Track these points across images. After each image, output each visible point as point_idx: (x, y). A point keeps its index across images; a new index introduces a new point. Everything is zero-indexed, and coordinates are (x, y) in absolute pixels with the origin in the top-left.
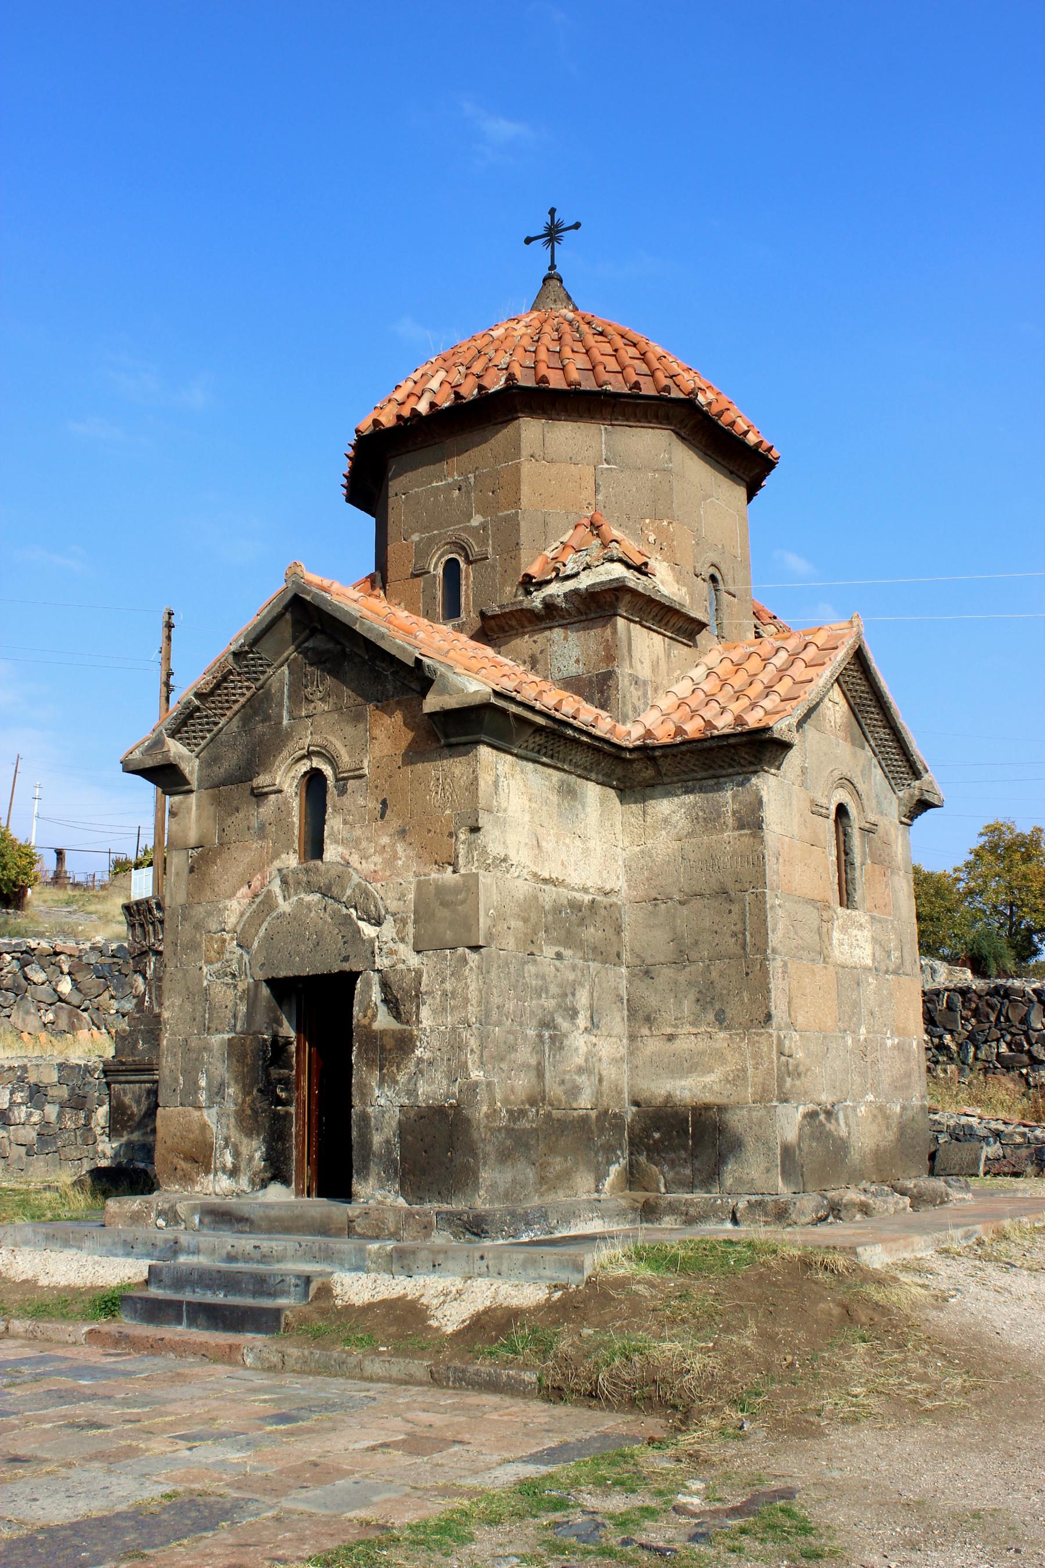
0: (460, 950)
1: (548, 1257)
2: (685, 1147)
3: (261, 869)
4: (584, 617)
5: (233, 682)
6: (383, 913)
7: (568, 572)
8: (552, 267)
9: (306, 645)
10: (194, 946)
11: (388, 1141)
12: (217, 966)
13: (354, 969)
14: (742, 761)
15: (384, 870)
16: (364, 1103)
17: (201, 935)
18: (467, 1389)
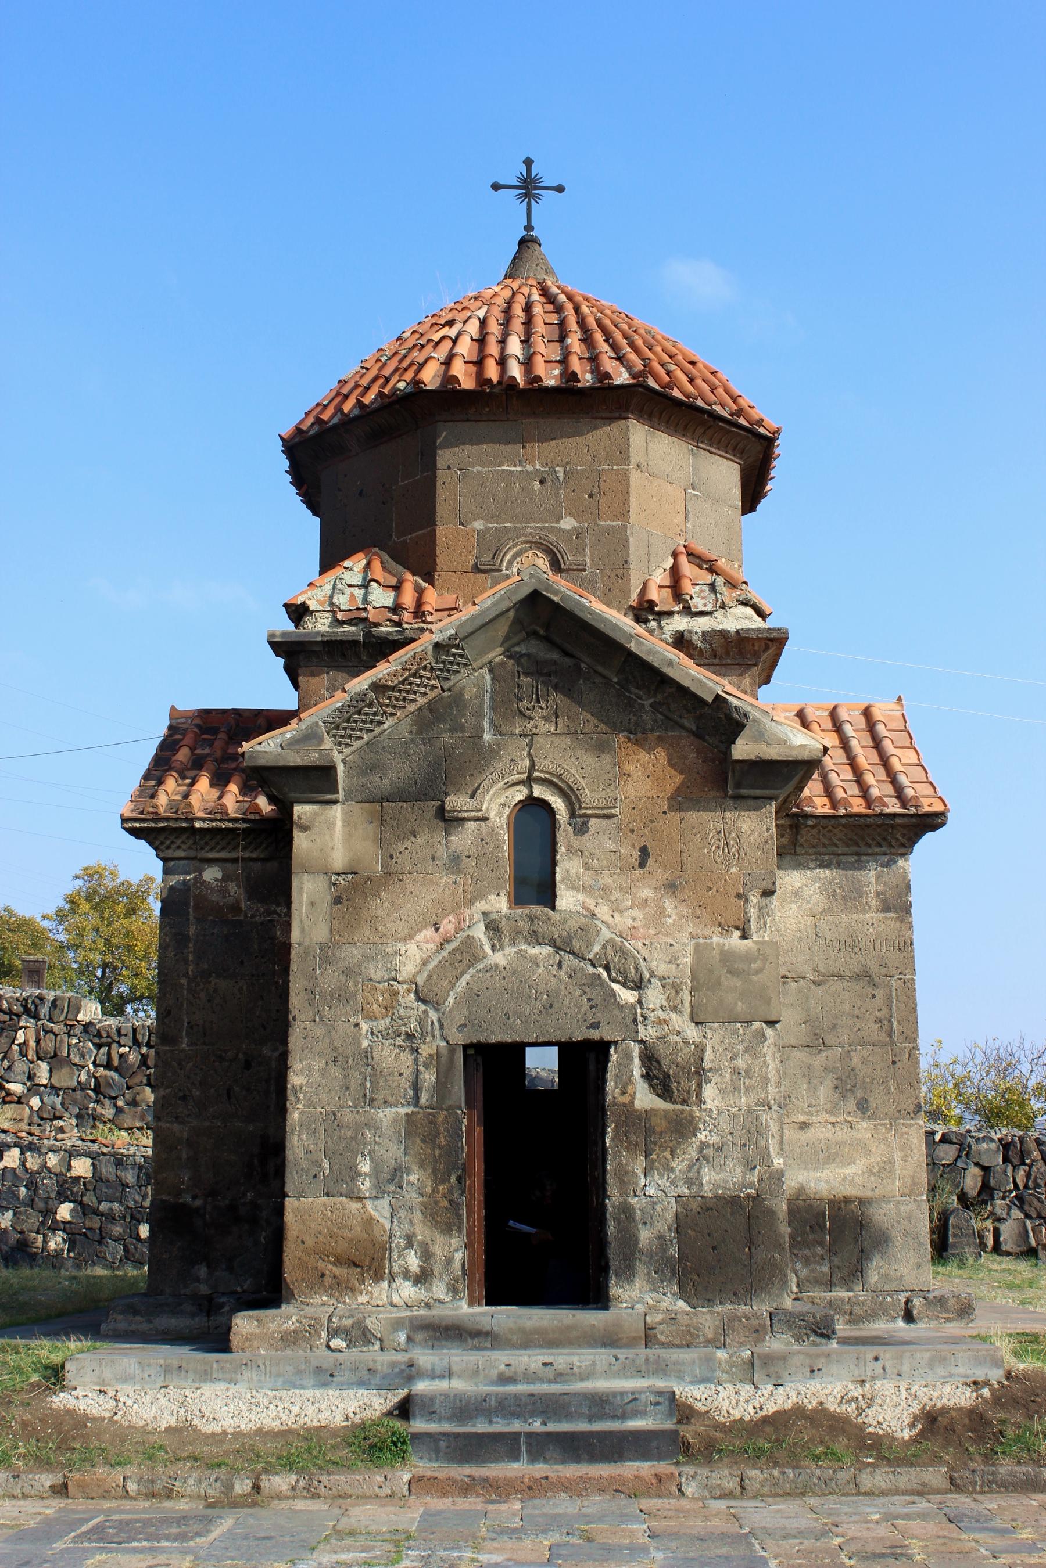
0: (757, 1025)
1: (961, 1354)
2: (821, 1243)
3: (455, 909)
4: (716, 661)
5: (421, 677)
6: (648, 976)
7: (701, 608)
8: (529, 227)
9: (517, 649)
10: (343, 996)
11: (661, 1237)
12: (383, 1023)
13: (607, 1038)
14: (893, 842)
15: (646, 926)
16: (623, 1192)
17: (356, 984)
18: (1000, 1492)
